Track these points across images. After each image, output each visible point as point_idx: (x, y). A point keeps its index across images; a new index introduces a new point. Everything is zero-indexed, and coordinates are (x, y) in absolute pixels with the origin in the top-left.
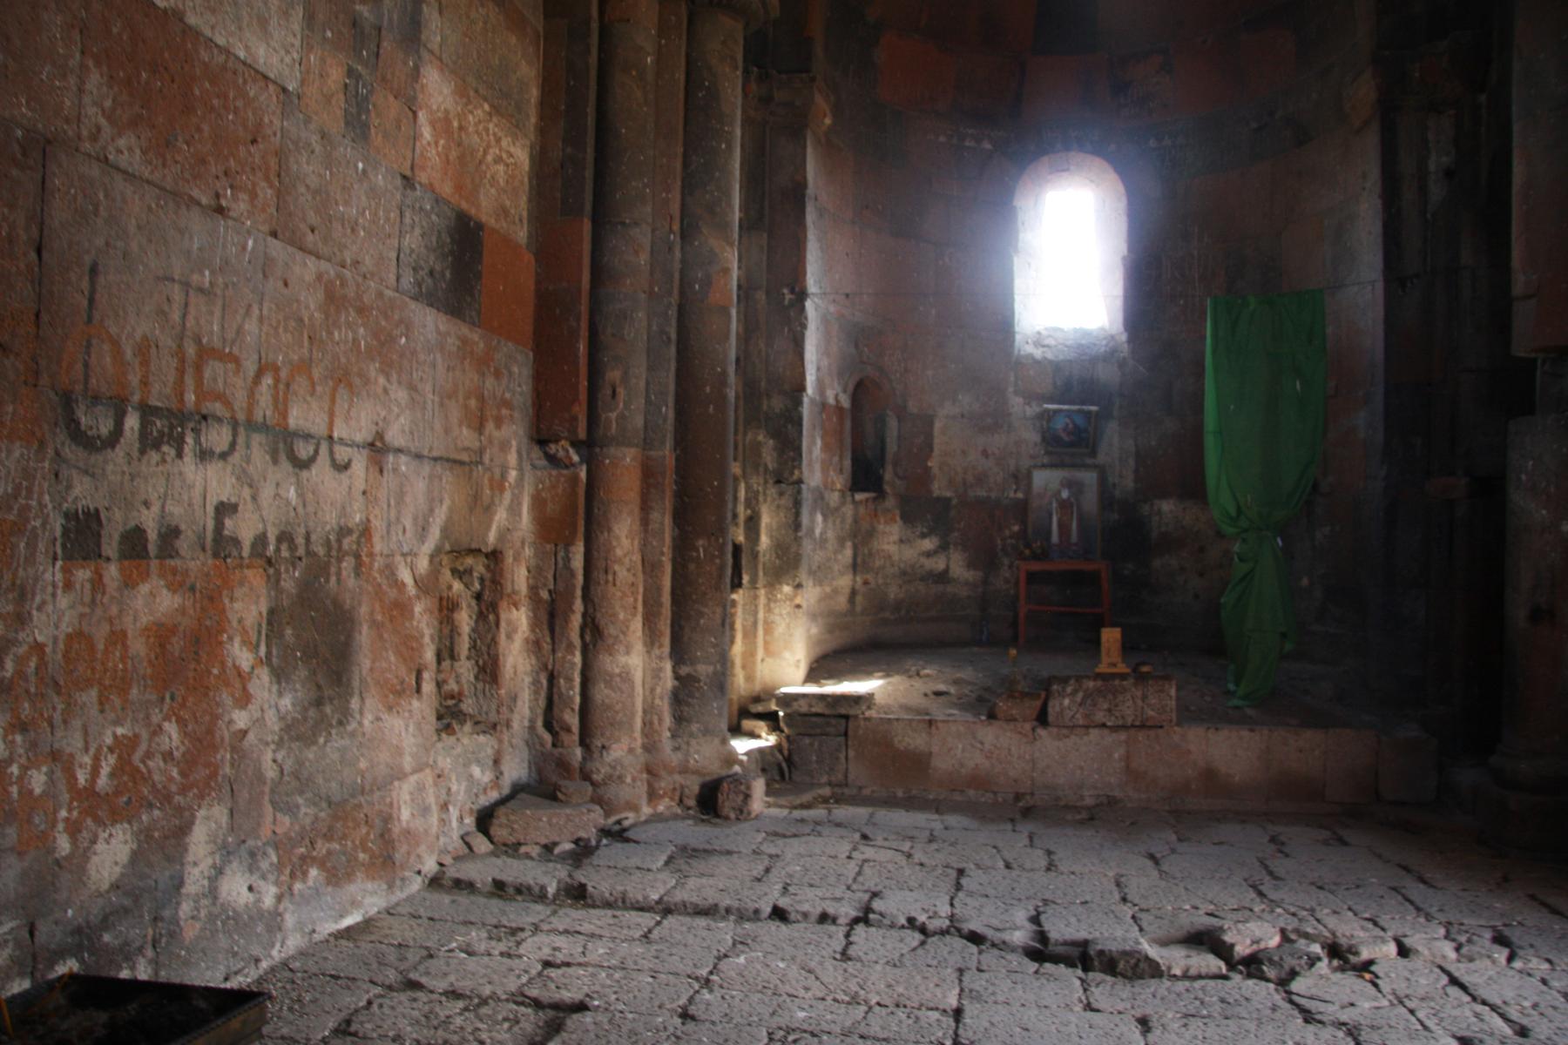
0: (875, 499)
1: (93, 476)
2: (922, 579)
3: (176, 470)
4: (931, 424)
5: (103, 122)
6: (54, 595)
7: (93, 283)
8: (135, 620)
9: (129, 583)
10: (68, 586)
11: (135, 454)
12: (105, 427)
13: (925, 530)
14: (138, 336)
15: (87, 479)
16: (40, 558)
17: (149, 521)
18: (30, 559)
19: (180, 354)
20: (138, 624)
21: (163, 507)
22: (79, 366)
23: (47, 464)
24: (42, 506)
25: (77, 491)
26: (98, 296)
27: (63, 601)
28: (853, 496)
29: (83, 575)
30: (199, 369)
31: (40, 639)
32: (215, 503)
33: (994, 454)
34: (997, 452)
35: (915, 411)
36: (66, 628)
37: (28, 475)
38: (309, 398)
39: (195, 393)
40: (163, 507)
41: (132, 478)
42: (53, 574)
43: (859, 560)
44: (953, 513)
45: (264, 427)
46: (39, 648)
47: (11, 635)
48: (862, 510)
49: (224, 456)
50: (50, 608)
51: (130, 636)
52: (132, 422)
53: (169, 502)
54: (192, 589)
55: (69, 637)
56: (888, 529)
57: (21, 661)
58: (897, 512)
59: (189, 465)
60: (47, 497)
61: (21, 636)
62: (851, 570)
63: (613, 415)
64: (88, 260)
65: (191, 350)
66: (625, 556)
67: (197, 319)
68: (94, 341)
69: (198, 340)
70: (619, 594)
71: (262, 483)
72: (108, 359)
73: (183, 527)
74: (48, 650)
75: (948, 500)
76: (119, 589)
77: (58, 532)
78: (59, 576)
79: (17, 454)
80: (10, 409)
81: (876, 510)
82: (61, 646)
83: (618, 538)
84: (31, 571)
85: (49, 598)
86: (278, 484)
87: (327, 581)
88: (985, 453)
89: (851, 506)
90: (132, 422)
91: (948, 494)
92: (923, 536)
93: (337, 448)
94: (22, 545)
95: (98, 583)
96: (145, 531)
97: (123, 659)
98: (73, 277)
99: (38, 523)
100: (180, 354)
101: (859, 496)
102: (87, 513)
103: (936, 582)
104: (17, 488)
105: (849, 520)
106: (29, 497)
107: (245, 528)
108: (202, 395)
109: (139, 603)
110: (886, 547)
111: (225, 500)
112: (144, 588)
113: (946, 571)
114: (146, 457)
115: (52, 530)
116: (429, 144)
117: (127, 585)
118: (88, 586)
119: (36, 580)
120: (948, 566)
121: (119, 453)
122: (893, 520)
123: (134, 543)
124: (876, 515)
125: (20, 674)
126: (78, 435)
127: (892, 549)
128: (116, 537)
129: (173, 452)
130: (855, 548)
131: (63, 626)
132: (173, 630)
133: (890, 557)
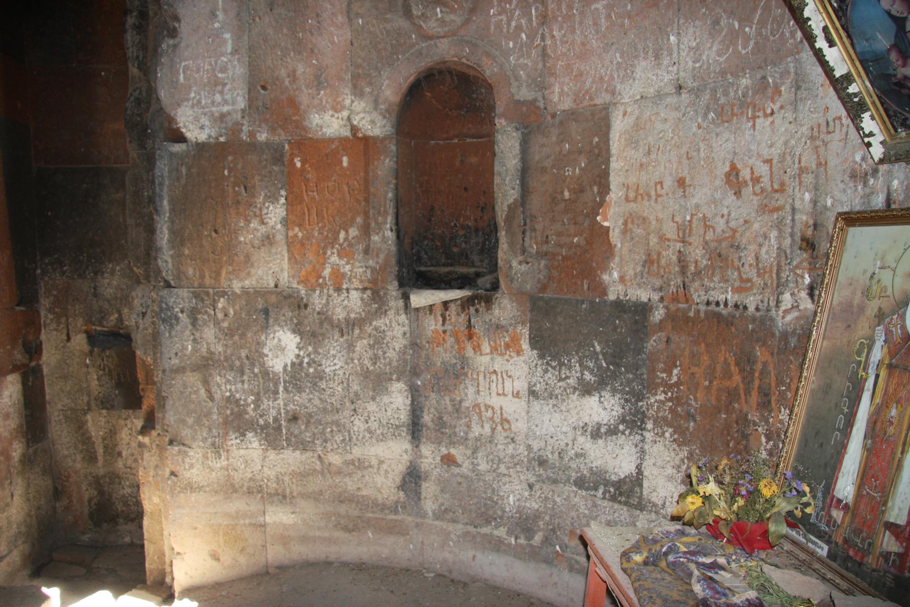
0: (466, 304)
2: (580, 483)
4: (602, 125)
13: (588, 376)
28: (406, 297)
33: (756, 180)
34: (763, 170)
35: (567, 104)
43: (427, 418)
44: (653, 343)
48: (432, 324)
56: (499, 364)
58: (524, 332)
62: (404, 432)
75: (643, 309)
81: (470, 326)
88: (733, 179)
89: (403, 318)
91: (643, 295)
92: (586, 390)
101: (421, 298)
103: (613, 499)
105: (399, 343)
110: (495, 401)
113: (637, 479)
120: (639, 468)
122: (513, 346)
124: (470, 337)
127: (513, 407)
130: (414, 392)
133: (505, 421)
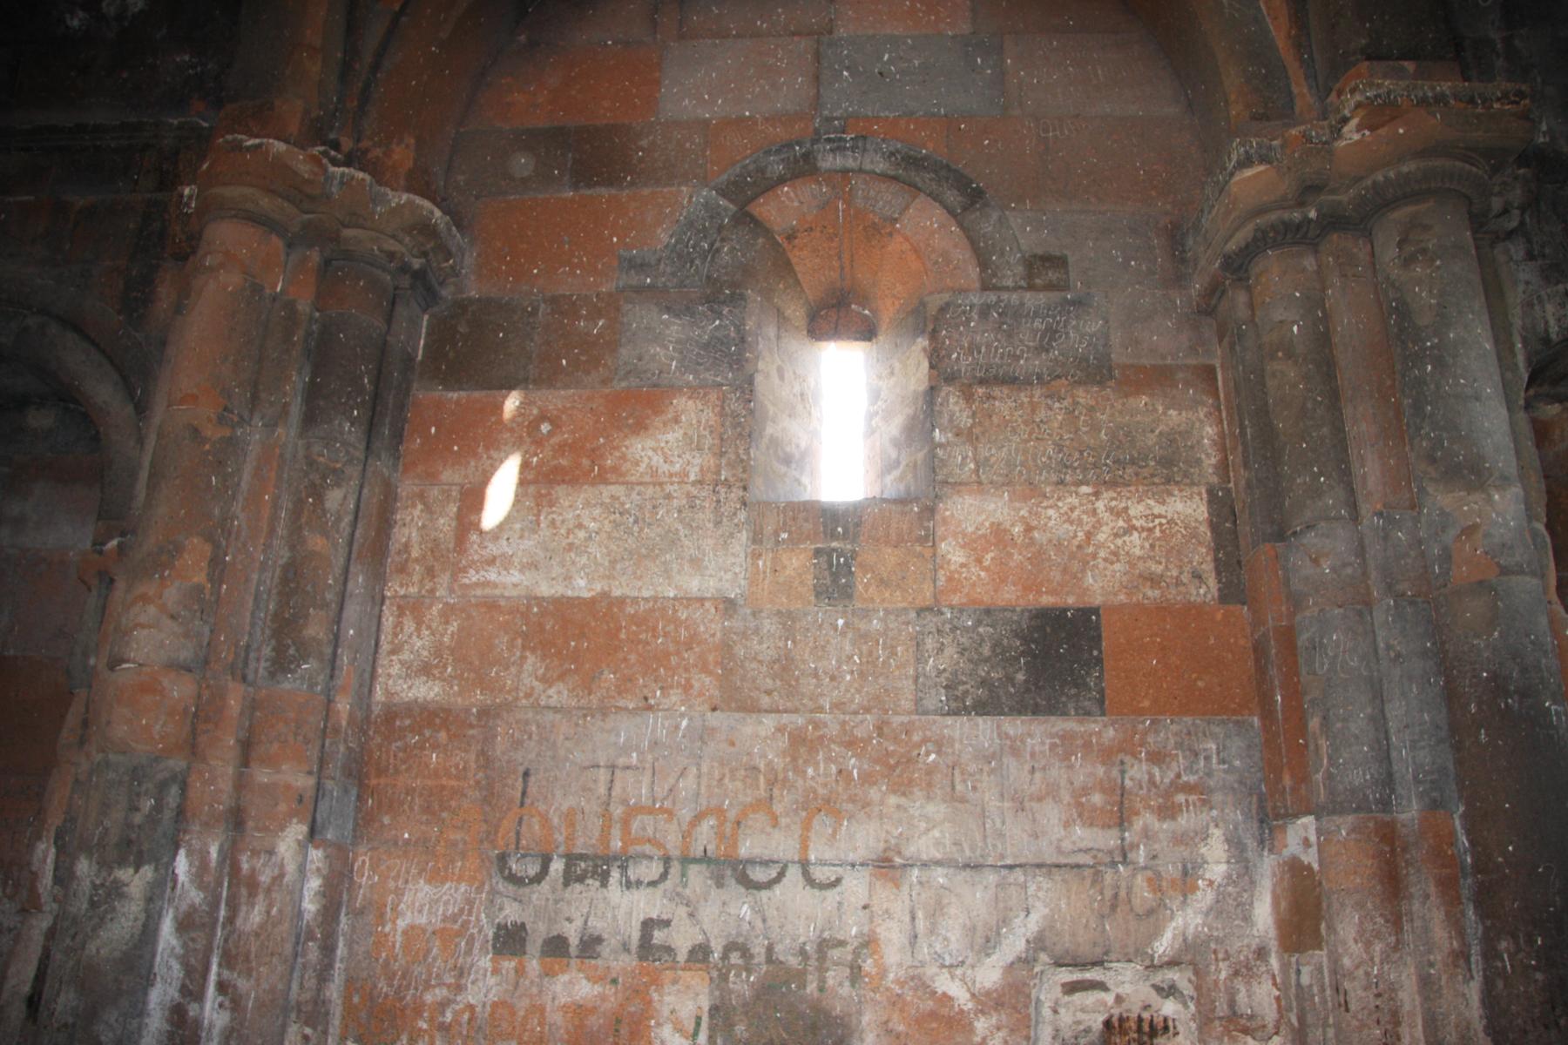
1: (520, 901)
3: (600, 896)
5: (536, 683)
6: (485, 976)
7: (525, 782)
8: (554, 999)
9: (549, 973)
10: (496, 971)
11: (560, 886)
12: (533, 869)
14: (564, 808)
15: (516, 905)
16: (475, 951)
17: (572, 933)
18: (469, 952)
19: (606, 815)
20: (557, 1002)
21: (586, 922)
22: (512, 834)
23: (484, 895)
24: (478, 920)
25: (507, 912)
26: (529, 790)
27: (491, 981)
29: (509, 965)
30: (626, 823)
31: (472, 1002)
32: (642, 918)
36: (493, 997)
37: (470, 902)
38: (769, 829)
39: (621, 840)
40: (586, 922)
41: (556, 902)
42: (485, 962)
45: (705, 859)
46: (471, 1007)
47: (452, 997)
49: (653, 884)
50: (481, 984)
51: (548, 1009)
52: (557, 866)
53: (591, 919)
54: (614, 981)
55: (495, 1005)
57: (457, 1014)
59: (614, 890)
60: (483, 915)
61: (459, 998)
63: (1319, 776)
64: (521, 769)
65: (618, 811)
66: (1357, 967)
67: (624, 789)
68: (525, 818)
69: (625, 802)
70: (1355, 1023)
71: (702, 903)
72: (537, 827)
73: (605, 936)
74: (478, 1009)
76: (540, 976)
77: (491, 934)
78: (489, 965)
79: (463, 890)
80: (459, 864)
82: (488, 1009)
83: (1344, 943)
84: (469, 960)
85: (480, 977)
86: (724, 904)
87: (803, 986)
90: (557, 866)
93: (812, 869)
94: (463, 944)
95: (520, 971)
96: (566, 939)
97: (541, 1024)
98: (510, 782)
99: (475, 931)
100: (606, 815)
102: (515, 924)
104: (462, 910)
106: (470, 913)
107: (682, 938)
108: (627, 839)
109: (558, 988)
111: (655, 917)
112: (565, 978)
114: (570, 888)
115: (486, 935)
116: (963, 565)
117: (547, 975)
118: (512, 972)
119: (472, 966)
121: (545, 886)
123: (556, 947)
125: (456, 1021)
126: (514, 879)
128: (540, 942)
129: (597, 884)
131: (491, 996)
132: (593, 1010)
